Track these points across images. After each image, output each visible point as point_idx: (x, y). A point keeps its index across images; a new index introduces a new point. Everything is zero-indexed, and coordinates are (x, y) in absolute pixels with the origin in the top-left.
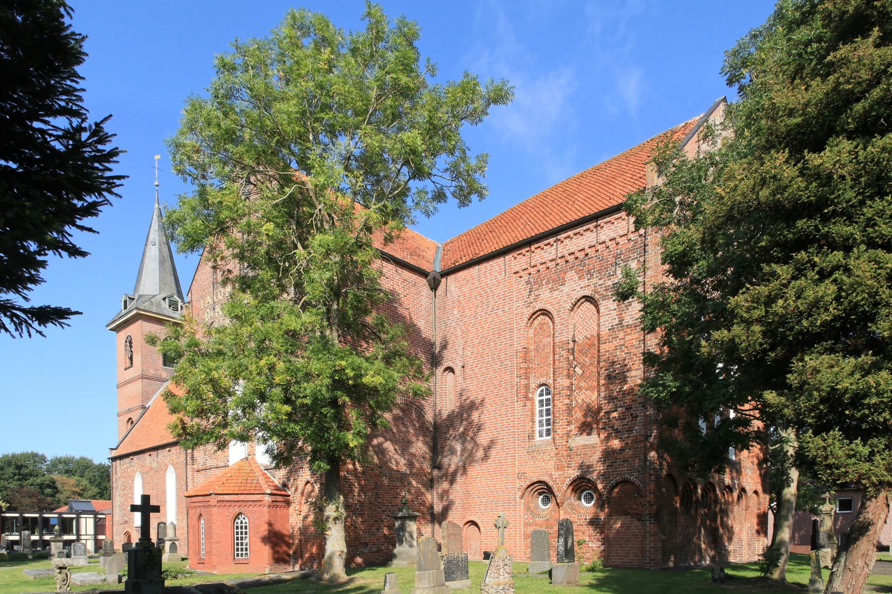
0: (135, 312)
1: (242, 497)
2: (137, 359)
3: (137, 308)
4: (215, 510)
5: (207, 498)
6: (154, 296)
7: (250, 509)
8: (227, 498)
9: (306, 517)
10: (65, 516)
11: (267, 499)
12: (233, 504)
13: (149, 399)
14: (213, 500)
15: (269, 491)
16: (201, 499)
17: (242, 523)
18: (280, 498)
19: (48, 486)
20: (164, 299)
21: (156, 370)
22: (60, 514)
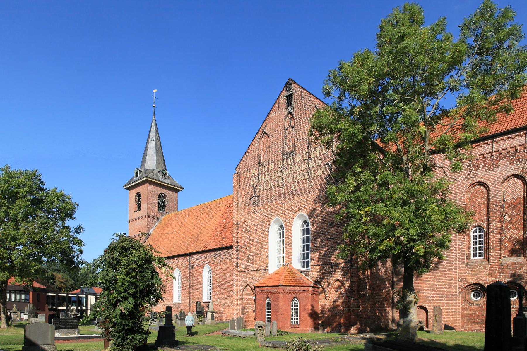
0: (145, 179)
1: (297, 288)
2: (144, 206)
3: (147, 177)
4: (281, 295)
5: (275, 288)
6: (154, 170)
7: (301, 295)
8: (288, 288)
9: (335, 301)
10: (80, 296)
11: (311, 289)
12: (291, 292)
13: (151, 229)
14: (280, 289)
15: (312, 285)
16: (269, 288)
17: (295, 303)
18: (316, 289)
19: (51, 278)
20: (159, 172)
21: (155, 213)
22: (77, 294)
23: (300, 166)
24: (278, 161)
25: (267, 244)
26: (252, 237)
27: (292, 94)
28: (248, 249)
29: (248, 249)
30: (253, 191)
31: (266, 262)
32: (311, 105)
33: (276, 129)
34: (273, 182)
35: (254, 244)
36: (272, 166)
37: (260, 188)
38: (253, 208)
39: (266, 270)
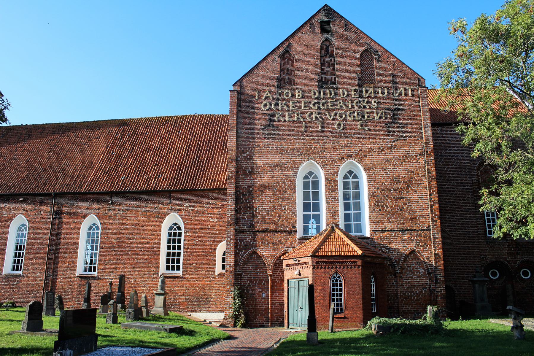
25: (292, 195)
32: (359, 40)
35: (268, 192)
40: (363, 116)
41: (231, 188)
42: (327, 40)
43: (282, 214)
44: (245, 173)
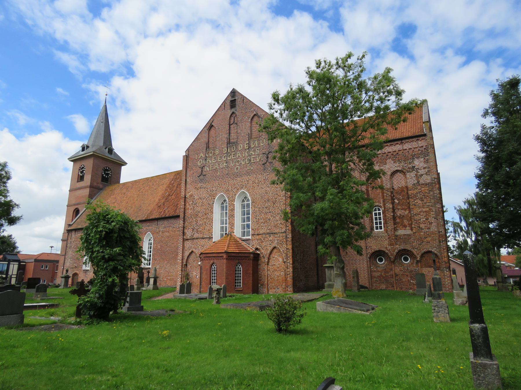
23: (242, 154)
24: (223, 148)
26: (198, 209)
27: (235, 100)
28: (194, 219)
29: (194, 219)
30: (201, 170)
31: (210, 231)
33: (222, 124)
34: (219, 165)
35: (200, 215)
36: (217, 152)
37: (207, 169)
38: (199, 185)
39: (211, 238)
40: (250, 160)
41: (182, 216)
42: (233, 113)
43: (206, 228)
44: (189, 205)
